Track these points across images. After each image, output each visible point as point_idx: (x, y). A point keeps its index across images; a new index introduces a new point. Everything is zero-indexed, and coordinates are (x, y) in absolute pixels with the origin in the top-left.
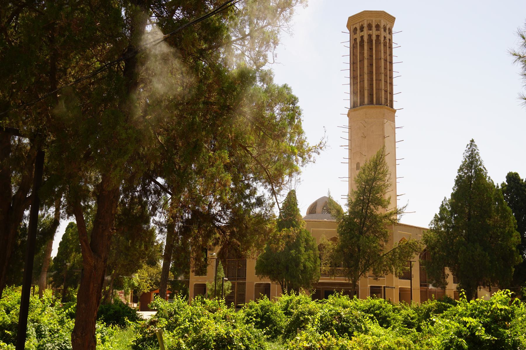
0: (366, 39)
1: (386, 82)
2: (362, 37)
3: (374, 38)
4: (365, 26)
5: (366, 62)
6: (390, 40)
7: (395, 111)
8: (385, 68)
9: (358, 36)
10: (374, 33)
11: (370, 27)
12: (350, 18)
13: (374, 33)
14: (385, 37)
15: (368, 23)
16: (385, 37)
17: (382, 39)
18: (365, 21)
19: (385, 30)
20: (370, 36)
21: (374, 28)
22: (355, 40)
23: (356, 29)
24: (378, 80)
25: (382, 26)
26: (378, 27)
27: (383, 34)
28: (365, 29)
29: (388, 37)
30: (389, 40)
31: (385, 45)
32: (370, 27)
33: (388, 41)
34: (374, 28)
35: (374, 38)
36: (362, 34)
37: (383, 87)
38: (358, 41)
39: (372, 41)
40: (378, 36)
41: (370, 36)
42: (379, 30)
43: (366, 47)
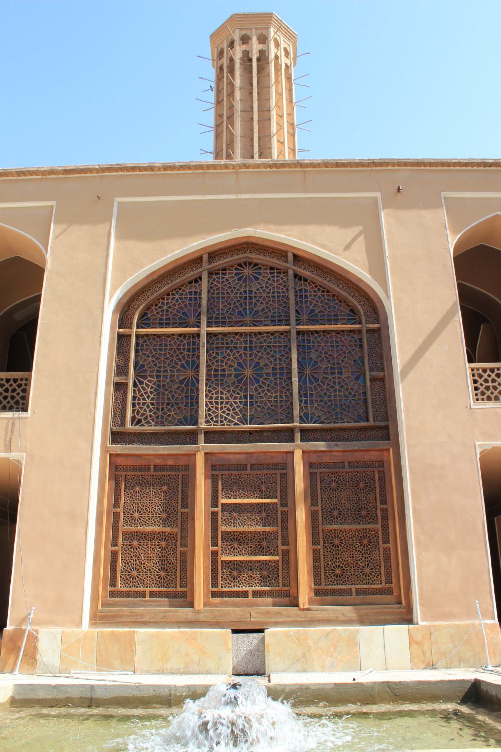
3: (254, 57)
5: (238, 94)
9: (225, 61)
10: (255, 47)
11: (245, 39)
12: (212, 36)
14: (276, 57)
15: (243, 32)
16: (276, 57)
17: (272, 56)
24: (265, 120)
26: (263, 39)
27: (273, 51)
29: (283, 60)
30: (286, 65)
33: (283, 67)
35: (254, 57)
37: (274, 129)
39: (250, 60)
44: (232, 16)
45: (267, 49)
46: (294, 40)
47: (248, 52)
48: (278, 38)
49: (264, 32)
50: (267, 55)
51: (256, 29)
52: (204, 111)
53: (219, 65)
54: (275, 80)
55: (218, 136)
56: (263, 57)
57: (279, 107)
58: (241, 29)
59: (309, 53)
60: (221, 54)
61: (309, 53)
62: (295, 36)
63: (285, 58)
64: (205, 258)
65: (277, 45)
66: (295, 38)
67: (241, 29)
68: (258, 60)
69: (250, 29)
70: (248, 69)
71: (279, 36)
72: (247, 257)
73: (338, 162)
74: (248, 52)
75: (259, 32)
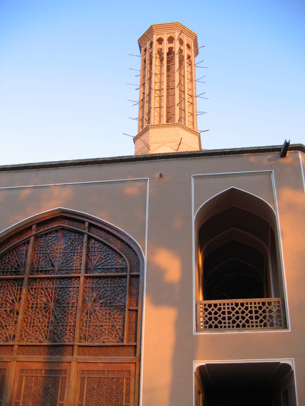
0: (155, 52)
1: (182, 99)
3: (165, 51)
10: (165, 47)
13: (165, 45)
14: (181, 51)
15: (159, 37)
16: (181, 51)
17: (176, 50)
21: (165, 41)
22: (145, 61)
24: (170, 95)
25: (176, 38)
26: (171, 40)
28: (155, 43)
29: (186, 52)
33: (186, 57)
34: (165, 41)
38: (147, 59)
42: (173, 43)
45: (174, 47)
46: (194, 38)
47: (162, 49)
48: (182, 38)
49: (173, 35)
50: (174, 51)
51: (167, 34)
52: (136, 90)
54: (180, 67)
55: (142, 107)
56: (171, 52)
58: (157, 35)
59: (204, 46)
60: (145, 50)
61: (204, 46)
62: (196, 35)
63: (188, 50)
64: (34, 227)
65: (181, 42)
66: (195, 36)
67: (157, 35)
68: (168, 54)
69: (163, 34)
70: (162, 60)
71: (184, 37)
72: (60, 226)
73: (121, 159)
74: (162, 49)
75: (169, 35)
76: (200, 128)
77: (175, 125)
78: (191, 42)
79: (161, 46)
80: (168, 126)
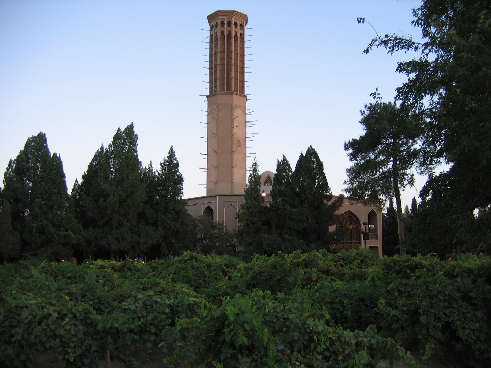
1: (236, 71)
2: (216, 33)
3: (226, 33)
4: (219, 24)
6: (242, 35)
7: (246, 97)
8: (236, 59)
9: (213, 32)
11: (223, 23)
14: (236, 33)
15: (221, 20)
16: (236, 33)
18: (219, 19)
19: (236, 27)
20: (222, 32)
21: (226, 25)
22: (212, 35)
23: (213, 26)
24: (229, 70)
25: (233, 22)
26: (229, 23)
29: (240, 32)
30: (241, 34)
31: (236, 40)
32: (223, 23)
34: (226, 25)
35: (226, 33)
36: (216, 30)
39: (224, 36)
40: (229, 33)
41: (222, 32)
43: (219, 42)
44: (217, 12)
47: (224, 31)
49: (230, 20)
53: (211, 34)
57: (236, 59)
76: (246, 92)
77: (231, 94)
78: (243, 22)
79: (222, 29)
80: (227, 94)
